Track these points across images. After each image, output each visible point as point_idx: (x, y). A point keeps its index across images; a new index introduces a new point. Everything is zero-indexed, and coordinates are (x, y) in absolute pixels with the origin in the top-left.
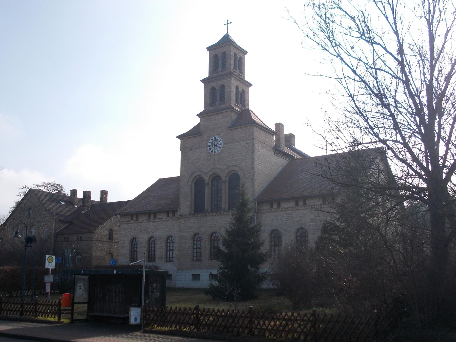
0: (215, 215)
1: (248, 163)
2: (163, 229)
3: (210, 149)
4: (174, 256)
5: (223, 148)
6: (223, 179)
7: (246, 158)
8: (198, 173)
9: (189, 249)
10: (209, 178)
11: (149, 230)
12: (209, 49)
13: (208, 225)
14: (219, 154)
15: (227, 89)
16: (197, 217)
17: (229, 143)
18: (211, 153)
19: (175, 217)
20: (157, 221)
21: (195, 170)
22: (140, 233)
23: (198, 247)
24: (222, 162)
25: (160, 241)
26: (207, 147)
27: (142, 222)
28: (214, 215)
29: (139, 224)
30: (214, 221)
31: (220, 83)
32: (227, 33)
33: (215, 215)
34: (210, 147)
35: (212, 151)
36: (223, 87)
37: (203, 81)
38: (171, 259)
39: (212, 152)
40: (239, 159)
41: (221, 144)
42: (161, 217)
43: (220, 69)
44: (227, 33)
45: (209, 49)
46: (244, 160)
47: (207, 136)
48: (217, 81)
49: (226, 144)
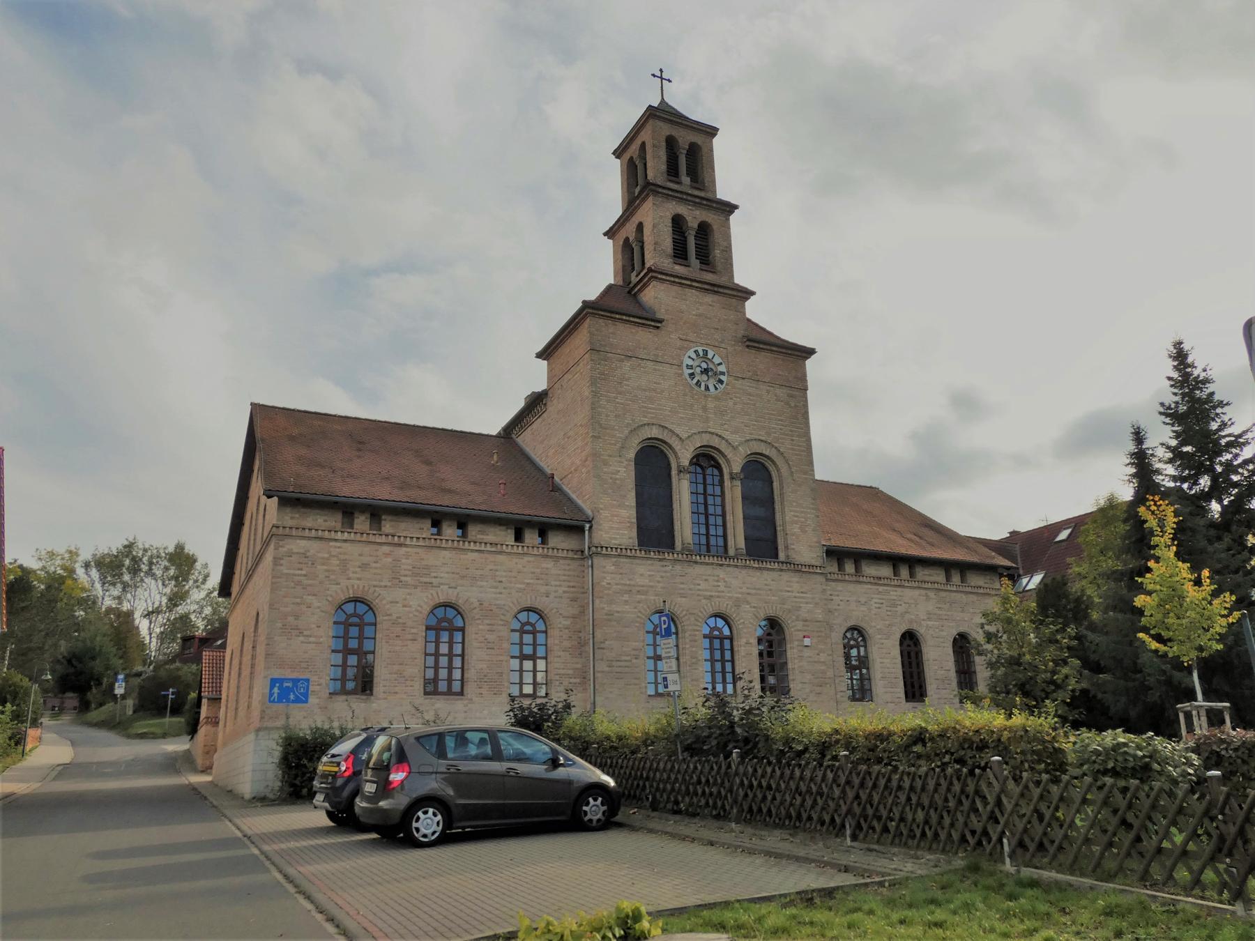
0: (721, 565)
2: (501, 582)
3: (692, 375)
7: (791, 431)
8: (655, 432)
9: (636, 658)
11: (435, 577)
13: (699, 590)
14: (717, 398)
16: (660, 560)
17: (743, 378)
18: (696, 388)
20: (472, 551)
21: (646, 420)
22: (389, 584)
23: (525, 652)
24: (728, 421)
25: (488, 622)
27: (400, 545)
28: (718, 564)
29: (386, 549)
30: (718, 581)
32: (663, 98)
33: (721, 565)
35: (698, 384)
40: (773, 428)
44: (663, 98)
48: (689, 205)
49: (737, 378)
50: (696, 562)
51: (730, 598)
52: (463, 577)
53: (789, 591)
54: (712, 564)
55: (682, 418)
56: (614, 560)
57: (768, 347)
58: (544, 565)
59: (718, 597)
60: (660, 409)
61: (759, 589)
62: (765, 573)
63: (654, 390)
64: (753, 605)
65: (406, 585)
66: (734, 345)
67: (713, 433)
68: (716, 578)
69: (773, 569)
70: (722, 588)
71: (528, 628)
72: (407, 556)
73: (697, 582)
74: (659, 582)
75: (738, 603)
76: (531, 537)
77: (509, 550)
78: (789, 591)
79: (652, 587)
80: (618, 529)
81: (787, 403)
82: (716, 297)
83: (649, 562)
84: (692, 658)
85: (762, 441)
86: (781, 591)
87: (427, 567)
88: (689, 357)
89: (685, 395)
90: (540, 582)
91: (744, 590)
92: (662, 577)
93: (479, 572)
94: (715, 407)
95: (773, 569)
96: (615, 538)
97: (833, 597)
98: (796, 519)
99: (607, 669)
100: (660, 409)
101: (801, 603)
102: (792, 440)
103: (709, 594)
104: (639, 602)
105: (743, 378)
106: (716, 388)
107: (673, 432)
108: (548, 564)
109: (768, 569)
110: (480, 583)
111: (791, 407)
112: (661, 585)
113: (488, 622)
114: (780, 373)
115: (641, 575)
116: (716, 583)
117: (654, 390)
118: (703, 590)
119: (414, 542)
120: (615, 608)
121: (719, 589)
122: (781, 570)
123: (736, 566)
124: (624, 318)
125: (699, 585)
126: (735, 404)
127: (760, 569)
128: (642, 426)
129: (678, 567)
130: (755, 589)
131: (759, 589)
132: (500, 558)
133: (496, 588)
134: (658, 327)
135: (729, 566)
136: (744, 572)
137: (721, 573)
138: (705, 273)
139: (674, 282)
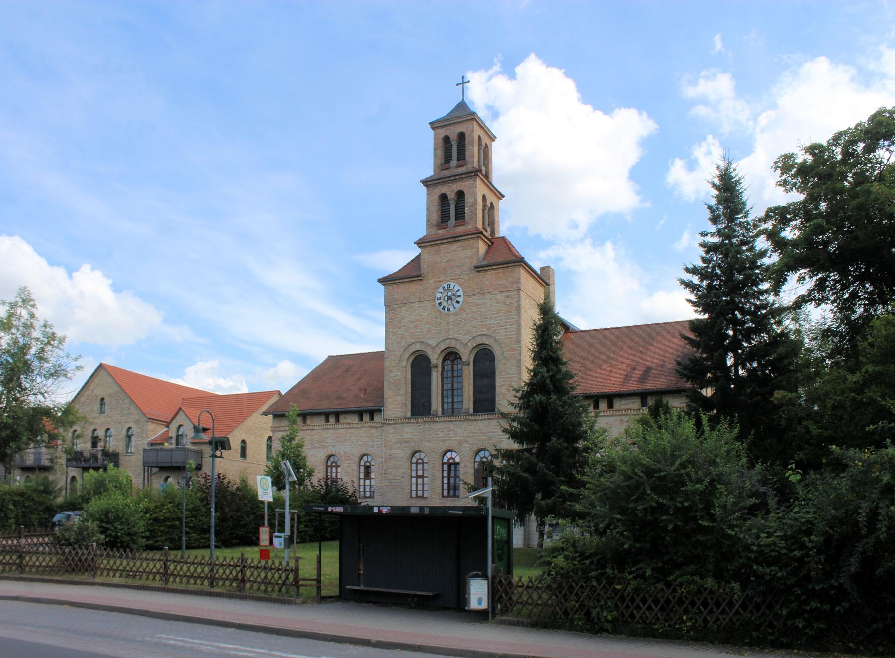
0: (451, 421)
1: (511, 331)
3: (440, 304)
4: (426, 487)
5: (463, 303)
6: (464, 358)
7: (506, 322)
8: (417, 347)
10: (439, 355)
12: (434, 125)
14: (456, 314)
15: (468, 199)
16: (417, 423)
17: (474, 295)
18: (442, 311)
21: (412, 341)
24: (463, 327)
25: (347, 462)
26: (434, 300)
27: (313, 429)
28: (449, 421)
29: (308, 432)
30: (450, 431)
31: (456, 187)
32: (463, 100)
33: (451, 421)
34: (439, 302)
35: (444, 308)
36: (461, 194)
37: (425, 183)
38: (420, 494)
39: (444, 310)
40: (493, 324)
41: (460, 296)
42: (348, 421)
43: (454, 163)
44: (463, 100)
45: (434, 125)
46: (502, 326)
47: (435, 282)
48: (449, 183)
49: (470, 296)
50: (436, 422)
51: (456, 440)
52: (337, 442)
53: (495, 432)
54: (446, 421)
55: (434, 333)
56: (393, 425)
57: (490, 268)
58: (372, 431)
59: (449, 440)
60: (421, 332)
61: (475, 433)
62: (480, 422)
63: (419, 321)
64: (470, 443)
65: (316, 448)
66: (469, 274)
67: (452, 338)
68: (448, 429)
69: (485, 419)
70: (452, 435)
71: (420, 461)
72: (316, 434)
73: (437, 433)
74: (416, 435)
75: (461, 443)
76: (366, 417)
77: (356, 425)
78: (495, 432)
79: (412, 438)
80: (396, 408)
81: (505, 303)
82: (459, 244)
83: (411, 425)
84: (433, 476)
85: (484, 335)
86: (490, 432)
87: (324, 439)
89: (436, 318)
90: (370, 440)
91: (466, 434)
92: (418, 432)
93: (344, 438)
94: (455, 320)
95: (485, 419)
96: (395, 414)
98: (504, 383)
99: (388, 484)
100: (421, 332)
101: (502, 438)
102: (506, 329)
103: (443, 439)
104: (406, 448)
105: (474, 295)
106: (455, 308)
107: (428, 344)
108: (374, 431)
109: (481, 420)
110: (344, 444)
111: (507, 305)
112: (417, 437)
113: (347, 462)
114: (500, 283)
115: (407, 432)
116: (448, 432)
117: (419, 321)
118: (440, 437)
119: (318, 427)
120: (393, 452)
121: (450, 435)
122: (490, 419)
123: (460, 421)
124: (401, 281)
125: (438, 434)
126: (467, 314)
127: (476, 420)
128: (410, 345)
129: (427, 425)
130: (473, 433)
131: (475, 433)
132: (352, 430)
133: (350, 445)
134: (421, 280)
135: (456, 421)
136: (465, 423)
137: (451, 425)
138: (457, 228)
139: (431, 245)
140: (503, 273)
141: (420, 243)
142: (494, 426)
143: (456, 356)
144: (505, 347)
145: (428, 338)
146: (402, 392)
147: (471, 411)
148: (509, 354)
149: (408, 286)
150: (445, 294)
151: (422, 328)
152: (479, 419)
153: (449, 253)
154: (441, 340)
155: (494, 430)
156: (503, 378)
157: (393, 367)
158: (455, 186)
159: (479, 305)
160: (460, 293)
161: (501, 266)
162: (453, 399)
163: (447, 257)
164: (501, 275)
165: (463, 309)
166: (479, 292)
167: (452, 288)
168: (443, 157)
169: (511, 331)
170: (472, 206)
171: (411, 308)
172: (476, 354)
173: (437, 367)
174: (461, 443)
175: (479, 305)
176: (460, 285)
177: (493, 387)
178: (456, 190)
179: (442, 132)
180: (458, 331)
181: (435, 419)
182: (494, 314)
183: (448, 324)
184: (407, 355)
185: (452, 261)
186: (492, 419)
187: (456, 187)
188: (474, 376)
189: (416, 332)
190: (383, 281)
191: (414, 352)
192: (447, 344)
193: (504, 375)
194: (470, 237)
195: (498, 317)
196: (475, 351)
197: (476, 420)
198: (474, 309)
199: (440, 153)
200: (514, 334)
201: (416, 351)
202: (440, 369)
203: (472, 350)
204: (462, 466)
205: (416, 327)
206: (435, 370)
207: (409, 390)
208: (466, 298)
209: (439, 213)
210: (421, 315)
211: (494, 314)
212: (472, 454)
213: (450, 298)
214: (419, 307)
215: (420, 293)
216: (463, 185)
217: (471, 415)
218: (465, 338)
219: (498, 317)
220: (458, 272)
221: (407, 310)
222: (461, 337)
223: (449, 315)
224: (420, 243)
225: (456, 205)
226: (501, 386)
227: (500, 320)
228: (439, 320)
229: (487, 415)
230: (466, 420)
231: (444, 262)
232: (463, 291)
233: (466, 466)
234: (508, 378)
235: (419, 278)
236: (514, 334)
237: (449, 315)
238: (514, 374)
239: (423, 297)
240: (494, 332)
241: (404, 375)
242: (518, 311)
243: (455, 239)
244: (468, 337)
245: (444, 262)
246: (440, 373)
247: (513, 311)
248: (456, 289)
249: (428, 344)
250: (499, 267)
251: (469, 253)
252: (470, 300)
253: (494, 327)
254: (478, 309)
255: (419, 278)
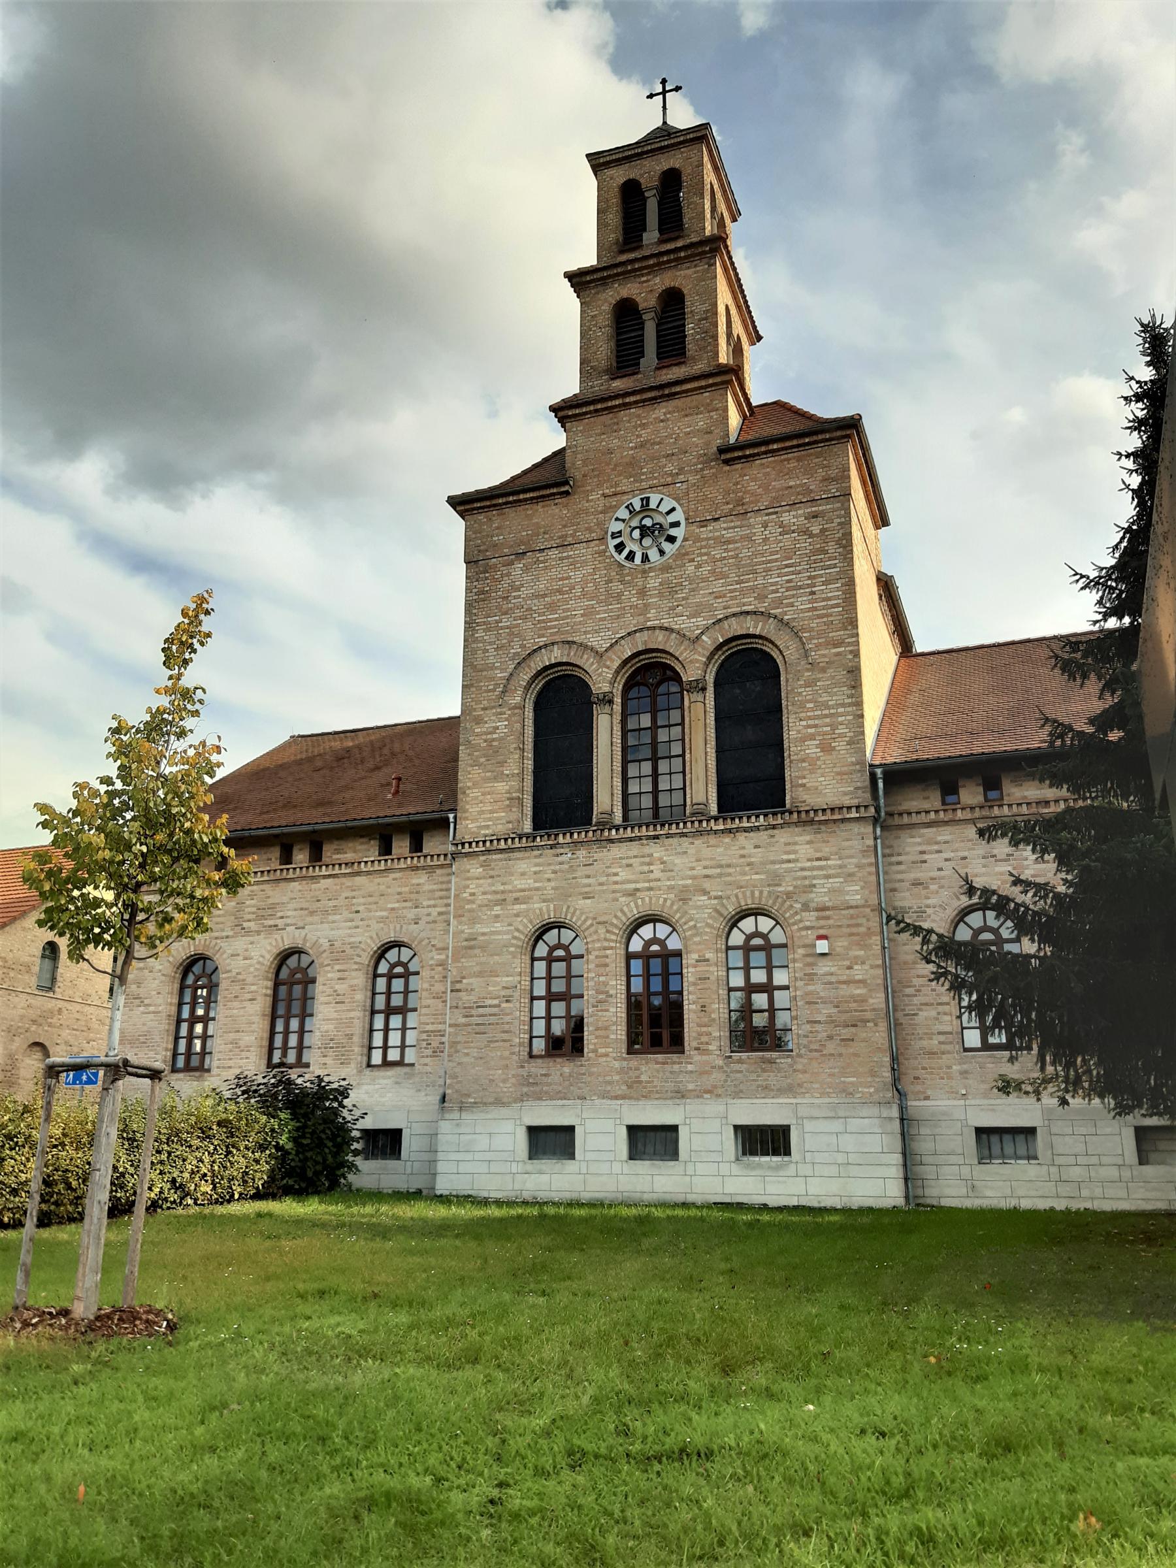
0: (656, 837)
1: (829, 599)
2: (358, 912)
3: (620, 547)
5: (685, 540)
6: (690, 674)
8: (556, 655)
9: (507, 1001)
10: (617, 672)
11: (282, 917)
12: (599, 162)
13: (616, 883)
14: (666, 568)
15: (694, 305)
16: (552, 847)
18: (627, 564)
19: (425, 857)
20: (325, 877)
21: (542, 641)
22: (231, 933)
24: (684, 598)
25: (337, 967)
26: (602, 539)
28: (649, 838)
30: (650, 864)
31: (660, 282)
33: (656, 837)
34: (617, 541)
35: (631, 556)
36: (673, 300)
37: (579, 280)
39: (633, 560)
40: (772, 584)
41: (676, 524)
42: (349, 856)
43: (651, 236)
45: (599, 162)
46: (800, 588)
47: (605, 496)
48: (643, 275)
49: (704, 523)
50: (611, 841)
51: (671, 888)
52: (312, 913)
53: (789, 861)
54: (640, 838)
55: (601, 619)
56: (482, 858)
57: (763, 449)
58: (415, 881)
59: (650, 889)
60: (567, 617)
61: (729, 866)
62: (741, 837)
63: (560, 591)
64: (713, 894)
65: (248, 932)
66: (702, 470)
67: (654, 628)
68: (647, 860)
69: (757, 828)
70: (657, 874)
72: (251, 896)
73: (614, 870)
74: (549, 880)
75: (684, 897)
76: (401, 846)
77: (369, 867)
78: (789, 861)
79: (537, 889)
80: (491, 812)
81: (807, 532)
82: (672, 404)
83: (536, 853)
84: (598, 992)
85: (748, 613)
86: (773, 862)
87: (273, 907)
88: (673, 509)
89: (610, 581)
90: (408, 904)
91: (699, 871)
92: (555, 872)
93: (331, 903)
94: (661, 584)
95: (757, 828)
96: (487, 827)
97: (926, 857)
98: (813, 730)
99: (463, 1020)
100: (567, 617)
101: (814, 878)
102: (813, 593)
103: (633, 886)
104: (517, 915)
105: (716, 520)
106: (662, 552)
107: (586, 647)
108: (421, 878)
109: (746, 830)
110: (331, 918)
111: (811, 536)
112: (553, 884)
113: (337, 967)
114: (792, 483)
115: (523, 874)
116: (646, 868)
117: (560, 591)
118: (623, 883)
119: (259, 878)
120: (479, 928)
121: (652, 876)
122: (774, 827)
123: (683, 835)
124: (511, 499)
125: (616, 874)
126: (698, 567)
127: (730, 831)
128: (535, 651)
129: (582, 853)
130: (721, 866)
131: (729, 866)
132: (359, 880)
133: (352, 920)
134: (567, 493)
135: (668, 836)
136: (698, 842)
137: (656, 850)
138: (665, 371)
139: (596, 411)
140: (799, 459)
141: (564, 412)
142: (786, 844)
143: (665, 673)
144: (811, 638)
145: (585, 633)
146: (512, 768)
147: (714, 809)
148: (824, 656)
149: (530, 512)
150: (635, 523)
151: (568, 610)
152: (738, 829)
153: (644, 426)
154: (622, 633)
155: (785, 857)
156: (810, 718)
157: (484, 709)
158: (657, 280)
159: (729, 542)
160: (678, 516)
161: (795, 442)
162: (655, 784)
163: (640, 436)
164: (793, 464)
165: (687, 554)
166: (732, 510)
167: (653, 505)
168: (620, 228)
169: (829, 599)
170: (706, 319)
171: (538, 561)
172: (722, 665)
173: (611, 702)
174: (684, 897)
175: (729, 542)
176: (677, 499)
177: (777, 745)
178: (660, 288)
179: (619, 175)
180: (673, 608)
181: (606, 833)
182: (776, 560)
183: (642, 593)
184: (525, 676)
185: (654, 443)
186: (782, 826)
187: (660, 282)
188: (717, 720)
189: (551, 620)
190: (463, 504)
191: (546, 668)
192: (641, 642)
193: (809, 710)
194: (703, 383)
195: (787, 566)
196: (720, 657)
197: (730, 831)
198: (717, 553)
199: (615, 218)
200: (837, 606)
201: (552, 666)
202: (617, 707)
203: (713, 654)
204: (689, 959)
205: (552, 607)
206: (607, 708)
207: (529, 764)
208: (693, 527)
209: (613, 344)
210: (569, 578)
211: (776, 560)
212: (720, 924)
213: (645, 531)
214: (561, 559)
215: (565, 526)
216: (682, 278)
217: (716, 819)
218: (690, 624)
219: (787, 566)
220: (670, 468)
221: (526, 569)
222: (682, 623)
223: (644, 572)
224: (564, 412)
225: (658, 325)
226: (803, 740)
227: (793, 573)
228: (616, 587)
229: (766, 815)
230: (700, 833)
231: (632, 449)
232: (684, 512)
233: (703, 960)
234: (826, 716)
235: (563, 489)
236: (837, 606)
237: (644, 572)
238: (843, 705)
239: (573, 535)
240: (779, 603)
241: (518, 726)
242: (844, 547)
243: (664, 393)
244: (701, 622)
245: (632, 449)
246: (617, 718)
247: (832, 548)
248: (664, 508)
249: (584, 647)
250: (788, 444)
251: (701, 422)
252: (704, 532)
253: (777, 591)
254: (726, 550)
255: (563, 489)
